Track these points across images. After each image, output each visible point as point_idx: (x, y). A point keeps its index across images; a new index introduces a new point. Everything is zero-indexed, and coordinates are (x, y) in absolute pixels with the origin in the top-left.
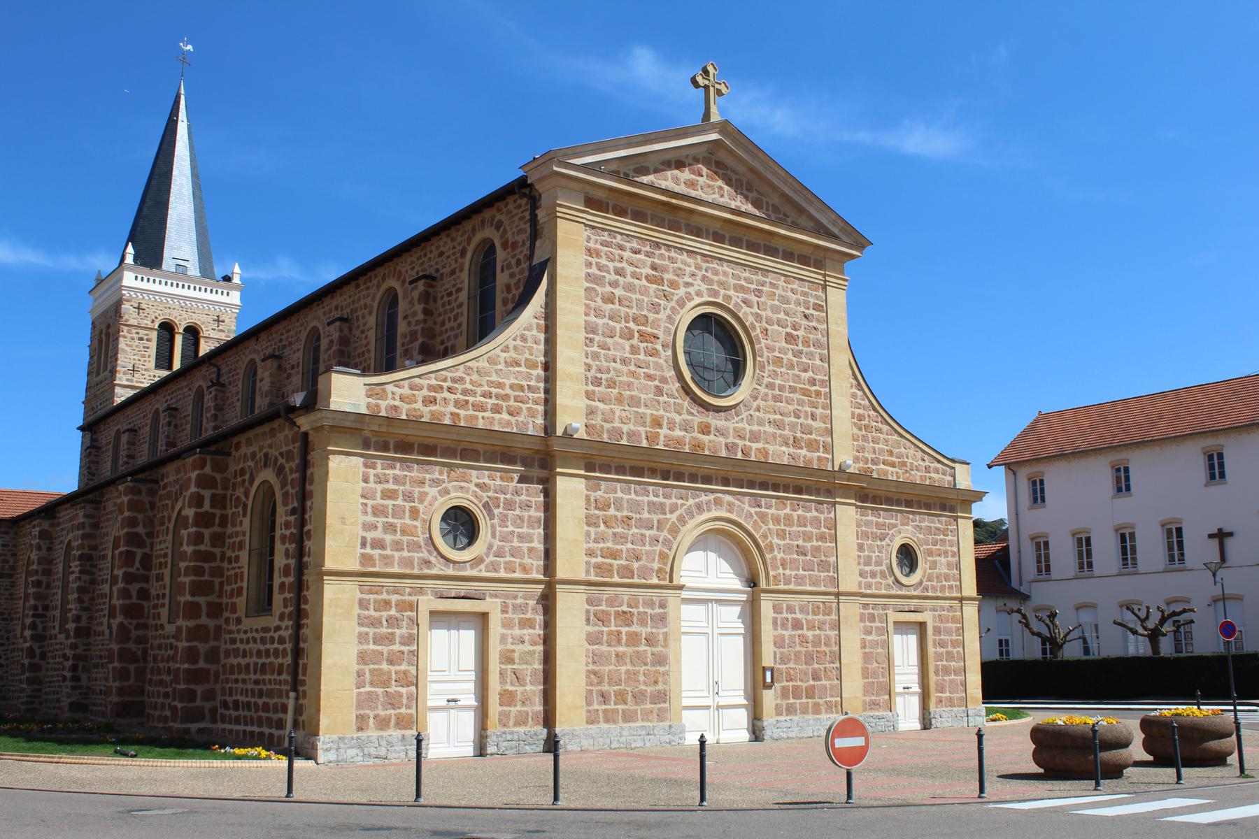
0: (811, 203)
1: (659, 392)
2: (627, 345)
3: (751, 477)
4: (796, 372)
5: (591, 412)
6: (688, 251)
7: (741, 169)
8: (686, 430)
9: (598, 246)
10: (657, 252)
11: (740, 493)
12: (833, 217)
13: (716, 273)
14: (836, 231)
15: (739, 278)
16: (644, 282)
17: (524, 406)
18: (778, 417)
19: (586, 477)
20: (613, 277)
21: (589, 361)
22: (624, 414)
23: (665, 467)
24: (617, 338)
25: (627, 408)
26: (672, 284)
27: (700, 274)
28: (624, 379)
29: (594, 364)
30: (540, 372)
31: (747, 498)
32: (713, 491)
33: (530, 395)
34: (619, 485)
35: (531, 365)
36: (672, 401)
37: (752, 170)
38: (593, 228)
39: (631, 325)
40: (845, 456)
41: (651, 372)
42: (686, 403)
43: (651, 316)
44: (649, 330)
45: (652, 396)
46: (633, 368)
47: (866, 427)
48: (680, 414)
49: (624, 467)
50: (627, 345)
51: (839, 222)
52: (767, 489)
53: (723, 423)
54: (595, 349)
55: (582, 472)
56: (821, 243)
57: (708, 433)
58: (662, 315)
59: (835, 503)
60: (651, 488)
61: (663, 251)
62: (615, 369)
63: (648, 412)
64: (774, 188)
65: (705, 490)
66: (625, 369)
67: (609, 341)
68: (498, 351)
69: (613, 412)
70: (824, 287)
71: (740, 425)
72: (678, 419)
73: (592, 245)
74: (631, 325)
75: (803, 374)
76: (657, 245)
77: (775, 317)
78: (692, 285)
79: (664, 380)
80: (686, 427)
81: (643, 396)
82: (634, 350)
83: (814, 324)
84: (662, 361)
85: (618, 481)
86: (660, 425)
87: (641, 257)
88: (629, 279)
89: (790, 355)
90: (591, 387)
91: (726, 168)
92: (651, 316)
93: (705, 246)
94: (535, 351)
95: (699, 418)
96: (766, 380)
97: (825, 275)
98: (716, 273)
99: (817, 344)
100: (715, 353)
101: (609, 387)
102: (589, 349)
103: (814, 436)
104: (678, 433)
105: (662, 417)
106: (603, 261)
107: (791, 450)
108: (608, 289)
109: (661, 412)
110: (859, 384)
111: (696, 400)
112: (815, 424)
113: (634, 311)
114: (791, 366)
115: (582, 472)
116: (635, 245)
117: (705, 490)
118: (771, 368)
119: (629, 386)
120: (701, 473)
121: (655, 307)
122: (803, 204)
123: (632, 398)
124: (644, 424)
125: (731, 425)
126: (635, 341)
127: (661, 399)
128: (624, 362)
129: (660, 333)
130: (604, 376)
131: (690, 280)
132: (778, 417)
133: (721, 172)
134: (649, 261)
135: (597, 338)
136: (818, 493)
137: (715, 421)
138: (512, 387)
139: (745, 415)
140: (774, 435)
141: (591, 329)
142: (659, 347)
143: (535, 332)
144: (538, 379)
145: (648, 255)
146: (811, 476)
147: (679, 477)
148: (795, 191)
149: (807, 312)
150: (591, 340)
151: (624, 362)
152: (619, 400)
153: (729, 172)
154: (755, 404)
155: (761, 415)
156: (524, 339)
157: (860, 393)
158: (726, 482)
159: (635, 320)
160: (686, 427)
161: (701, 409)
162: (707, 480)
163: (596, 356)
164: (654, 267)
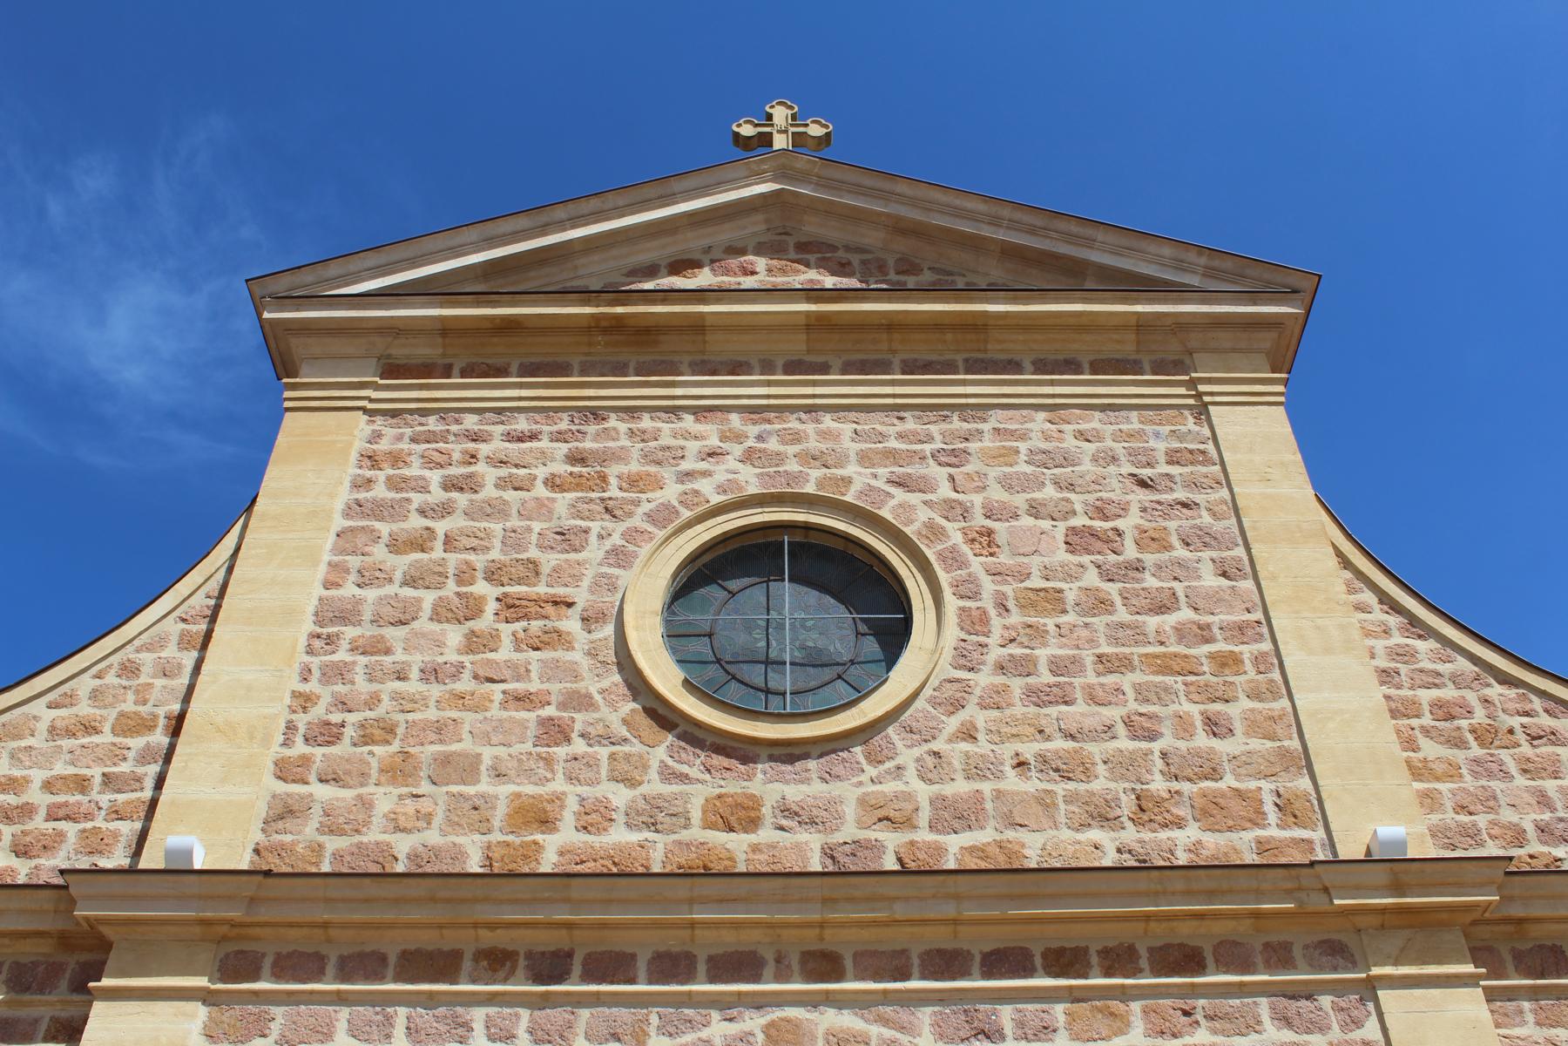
0: (1089, 243)
1: (555, 732)
2: (454, 636)
3: (940, 938)
4: (1122, 615)
5: (284, 813)
6: (695, 411)
7: (872, 238)
8: (653, 826)
9: (405, 446)
10: (592, 429)
11: (886, 998)
12: (1167, 251)
13: (796, 438)
14: (1195, 281)
15: (882, 437)
16: (541, 491)
17: (71, 829)
18: (1060, 744)
19: (206, 997)
20: (437, 495)
21: (313, 686)
22: (410, 806)
23: (548, 941)
24: (423, 624)
25: (425, 787)
26: (633, 482)
27: (737, 450)
28: (432, 714)
29: (325, 695)
30: (160, 738)
31: (926, 1015)
32: (759, 1003)
33: (105, 799)
34: (344, 1013)
35: (131, 725)
36: (603, 752)
37: (901, 228)
38: (394, 414)
39: (481, 587)
40: (1378, 811)
41: (534, 685)
42: (662, 749)
43: (549, 561)
44: (541, 589)
45: (528, 746)
46: (465, 684)
47: (1485, 736)
48: (631, 783)
49: (382, 959)
50: (454, 636)
51: (1192, 256)
52: (1029, 972)
53: (817, 788)
54: (342, 655)
55: (201, 982)
56: (1139, 308)
57: (752, 824)
58: (594, 552)
59: (1369, 989)
60: (478, 1015)
61: (612, 421)
62: (397, 697)
63: (505, 790)
64: (975, 244)
65: (723, 1004)
66: (435, 691)
67: (394, 634)
68: (38, 707)
69: (366, 804)
70: (1201, 411)
71: (890, 787)
72: (620, 796)
73: (384, 446)
74: (481, 587)
75: (1152, 622)
76: (596, 414)
77: (1020, 500)
78: (706, 474)
79: (581, 701)
80: (650, 816)
81: (487, 754)
82: (475, 643)
83: (1181, 494)
84: (577, 656)
85: (341, 999)
86: (546, 823)
87: (544, 443)
88: (489, 491)
89: (1092, 578)
90: (300, 748)
91: (834, 248)
92: (549, 561)
93: (752, 389)
94: (154, 696)
95: (705, 783)
96: (995, 653)
97: (1192, 383)
98: (796, 438)
99: (1206, 539)
100: (801, 615)
101: (366, 739)
102: (315, 662)
103: (1229, 781)
104: (619, 836)
105: (559, 798)
106: (414, 470)
107: (1130, 835)
108: (416, 522)
109: (559, 785)
110: (1413, 621)
111: (695, 736)
112: (1223, 747)
113: (495, 554)
114: (1102, 604)
115: (201, 982)
116: (522, 424)
117: (741, 1000)
118: (1015, 618)
119: (440, 730)
120: (705, 946)
121: (567, 539)
122: (1063, 249)
123: (445, 761)
124: (484, 826)
125: (848, 793)
126: (486, 622)
127: (561, 752)
128: (432, 673)
129: (581, 596)
130: (351, 718)
131: (703, 466)
132: (1060, 744)
133: (812, 258)
134: (563, 448)
135: (350, 632)
136: (1280, 956)
137: (768, 785)
138: (48, 786)
139: (907, 756)
140: (1045, 802)
141: (333, 615)
142: (571, 624)
143: (171, 652)
144: (144, 757)
145: (559, 437)
146: (1211, 895)
147: (610, 966)
148: (1032, 231)
149: (1145, 473)
150: (330, 640)
151: (432, 673)
152: (400, 771)
153: (840, 253)
154: (953, 723)
155: (983, 747)
156: (130, 669)
157: (1423, 646)
158: (824, 964)
159: (492, 576)
160: (650, 816)
161: (718, 760)
162: (738, 964)
163: (337, 673)
164: (576, 458)
